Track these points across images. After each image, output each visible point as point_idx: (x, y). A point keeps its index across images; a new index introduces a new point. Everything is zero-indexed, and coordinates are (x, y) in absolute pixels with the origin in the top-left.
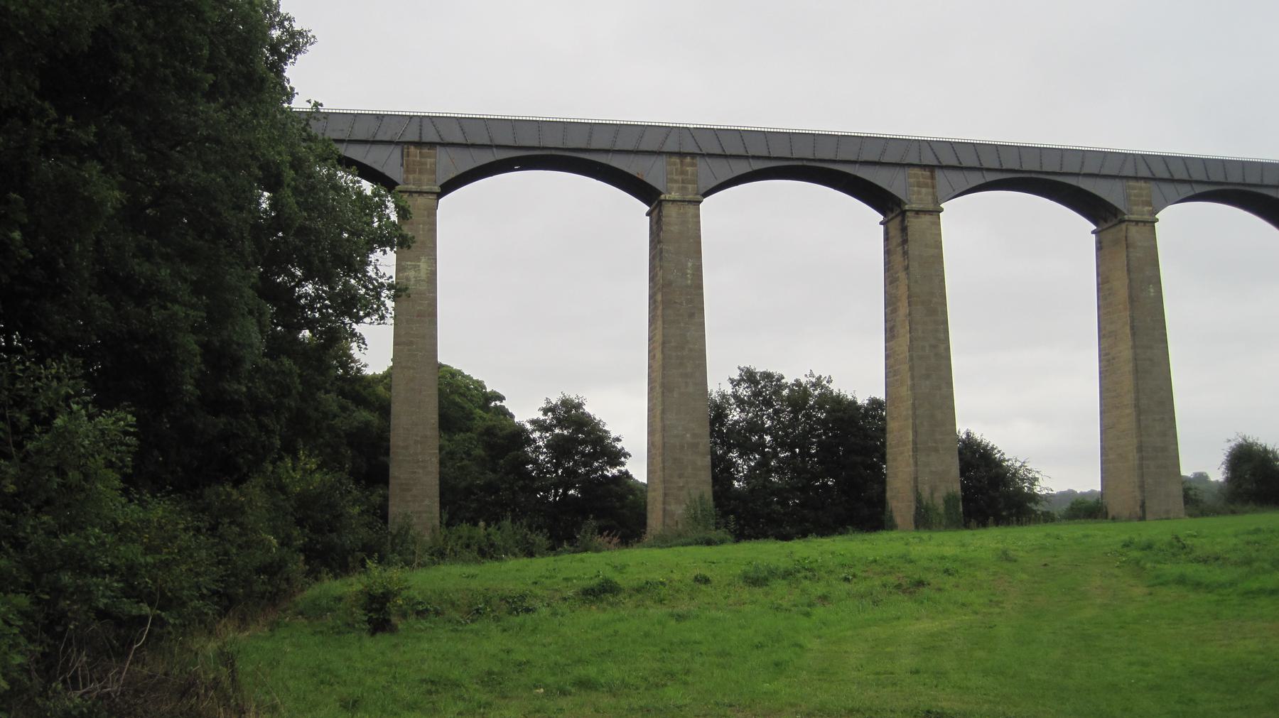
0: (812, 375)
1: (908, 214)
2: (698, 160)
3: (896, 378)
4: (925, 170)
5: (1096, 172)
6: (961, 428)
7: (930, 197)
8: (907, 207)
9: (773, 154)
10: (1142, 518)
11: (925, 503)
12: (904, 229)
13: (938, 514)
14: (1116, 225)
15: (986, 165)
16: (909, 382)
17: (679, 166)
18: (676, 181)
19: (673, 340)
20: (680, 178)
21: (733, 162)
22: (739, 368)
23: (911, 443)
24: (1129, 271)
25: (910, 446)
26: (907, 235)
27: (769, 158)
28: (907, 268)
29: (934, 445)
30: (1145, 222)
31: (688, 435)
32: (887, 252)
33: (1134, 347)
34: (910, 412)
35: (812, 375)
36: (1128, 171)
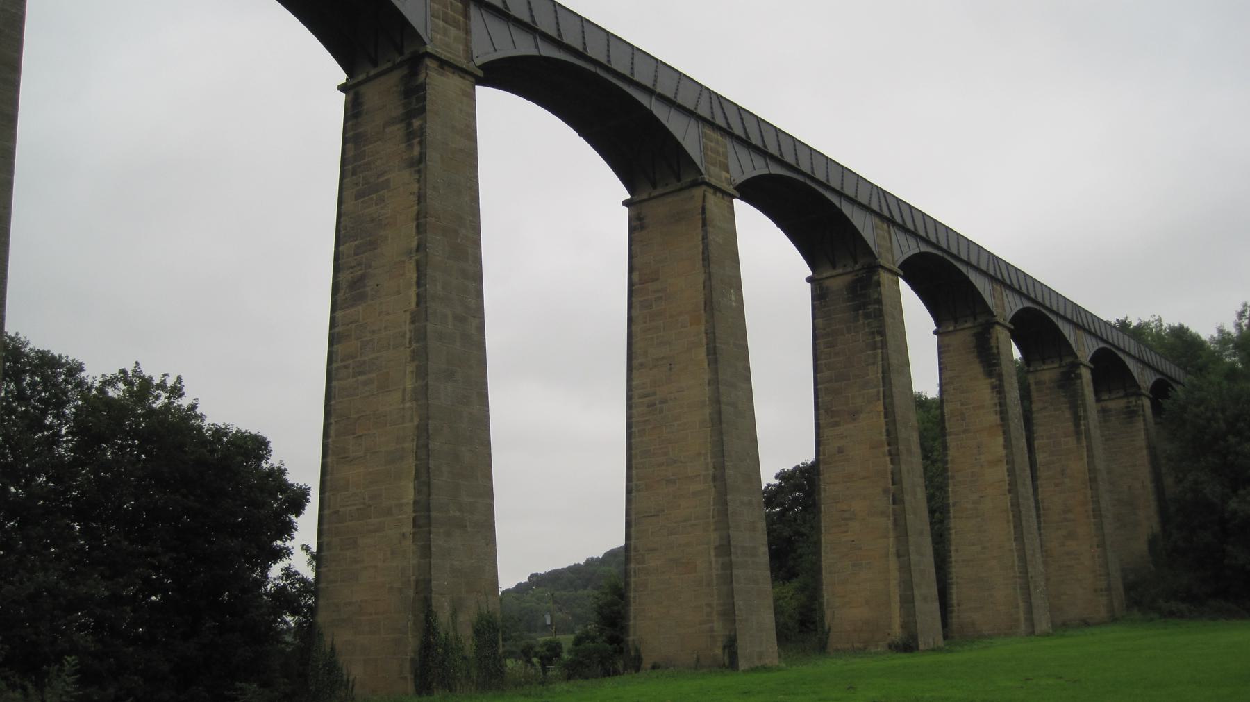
1: (428, 62)
3: (361, 378)
11: (443, 635)
13: (465, 658)
16: (409, 384)
24: (706, 259)
25: (409, 512)
28: (418, 164)
29: (458, 514)
30: (724, 193)
34: (410, 445)
36: (704, 111)
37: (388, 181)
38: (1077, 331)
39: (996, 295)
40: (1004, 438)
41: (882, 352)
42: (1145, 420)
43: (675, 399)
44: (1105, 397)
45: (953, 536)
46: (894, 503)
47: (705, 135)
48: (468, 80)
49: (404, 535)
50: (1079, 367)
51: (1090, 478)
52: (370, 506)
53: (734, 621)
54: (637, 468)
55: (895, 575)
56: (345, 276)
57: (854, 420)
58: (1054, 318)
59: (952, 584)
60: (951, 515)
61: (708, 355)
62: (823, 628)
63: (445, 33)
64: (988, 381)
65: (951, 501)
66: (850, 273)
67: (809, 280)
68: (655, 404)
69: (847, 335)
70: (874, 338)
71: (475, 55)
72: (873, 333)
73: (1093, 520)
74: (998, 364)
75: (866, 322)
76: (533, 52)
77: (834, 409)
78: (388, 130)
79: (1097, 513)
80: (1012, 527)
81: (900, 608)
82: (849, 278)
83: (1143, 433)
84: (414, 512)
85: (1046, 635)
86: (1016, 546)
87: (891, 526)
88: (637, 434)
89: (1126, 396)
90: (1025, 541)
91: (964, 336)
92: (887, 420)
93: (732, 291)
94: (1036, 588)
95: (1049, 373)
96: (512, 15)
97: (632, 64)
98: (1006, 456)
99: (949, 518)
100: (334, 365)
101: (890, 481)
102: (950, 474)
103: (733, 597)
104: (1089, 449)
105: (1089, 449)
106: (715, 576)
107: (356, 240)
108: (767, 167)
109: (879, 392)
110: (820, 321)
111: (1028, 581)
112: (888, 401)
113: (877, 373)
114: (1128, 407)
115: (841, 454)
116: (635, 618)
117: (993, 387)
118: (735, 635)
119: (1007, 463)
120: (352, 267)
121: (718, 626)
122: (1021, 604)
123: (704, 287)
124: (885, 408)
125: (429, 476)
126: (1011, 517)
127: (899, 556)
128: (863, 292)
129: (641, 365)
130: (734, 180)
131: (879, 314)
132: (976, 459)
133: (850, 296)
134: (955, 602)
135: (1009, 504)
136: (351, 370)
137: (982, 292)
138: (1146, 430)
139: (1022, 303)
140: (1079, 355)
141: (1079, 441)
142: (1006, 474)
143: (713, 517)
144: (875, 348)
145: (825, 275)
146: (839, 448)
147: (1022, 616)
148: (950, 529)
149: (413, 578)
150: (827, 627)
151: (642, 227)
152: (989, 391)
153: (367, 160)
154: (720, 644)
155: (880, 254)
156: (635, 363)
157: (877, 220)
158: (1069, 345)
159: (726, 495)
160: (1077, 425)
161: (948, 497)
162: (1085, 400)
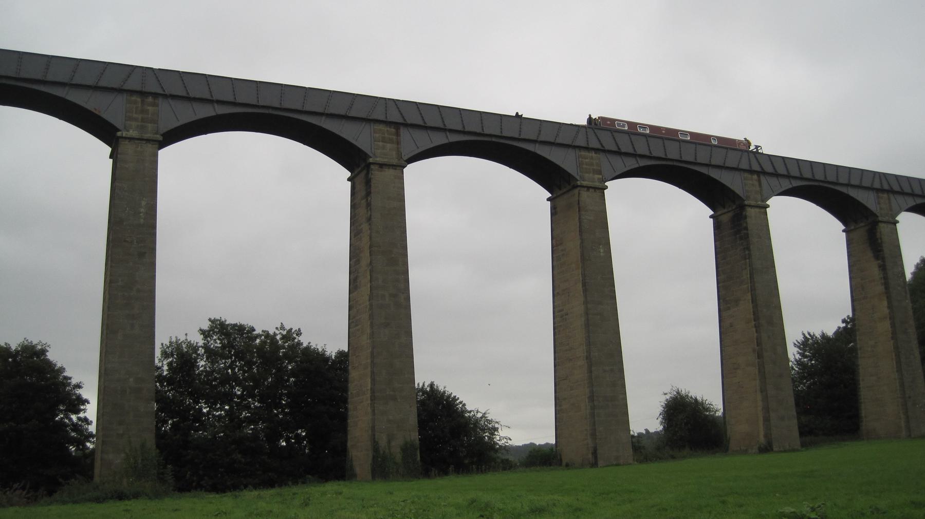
0: (282, 328)
1: (372, 167)
2: (160, 100)
3: (357, 328)
4: (390, 127)
5: (552, 140)
6: (422, 378)
7: (394, 153)
8: (371, 160)
9: (239, 100)
10: (594, 464)
11: (382, 452)
12: (368, 182)
15: (449, 127)
16: (369, 331)
17: (140, 105)
18: (136, 120)
19: (120, 279)
20: (140, 116)
21: (196, 105)
22: (210, 320)
23: (369, 392)
25: (369, 395)
26: (370, 186)
27: (234, 104)
28: (369, 219)
30: (595, 188)
31: (131, 380)
32: (353, 207)
33: (586, 302)
34: (369, 361)
35: (282, 328)
41: (749, 261)
60: (859, 356)
61: (582, 287)
71: (403, 155)
72: (744, 248)
77: (728, 299)
78: (362, 202)
82: (730, 214)
87: (757, 372)
93: (601, 246)
97: (520, 128)
101: (756, 343)
102: (857, 328)
110: (718, 243)
117: (880, 267)
119: (890, 318)
126: (894, 357)
127: (761, 392)
130: (605, 178)
131: (746, 237)
139: (915, 201)
144: (745, 259)
147: (903, 424)
150: (728, 436)
154: (591, 452)
157: (747, 175)
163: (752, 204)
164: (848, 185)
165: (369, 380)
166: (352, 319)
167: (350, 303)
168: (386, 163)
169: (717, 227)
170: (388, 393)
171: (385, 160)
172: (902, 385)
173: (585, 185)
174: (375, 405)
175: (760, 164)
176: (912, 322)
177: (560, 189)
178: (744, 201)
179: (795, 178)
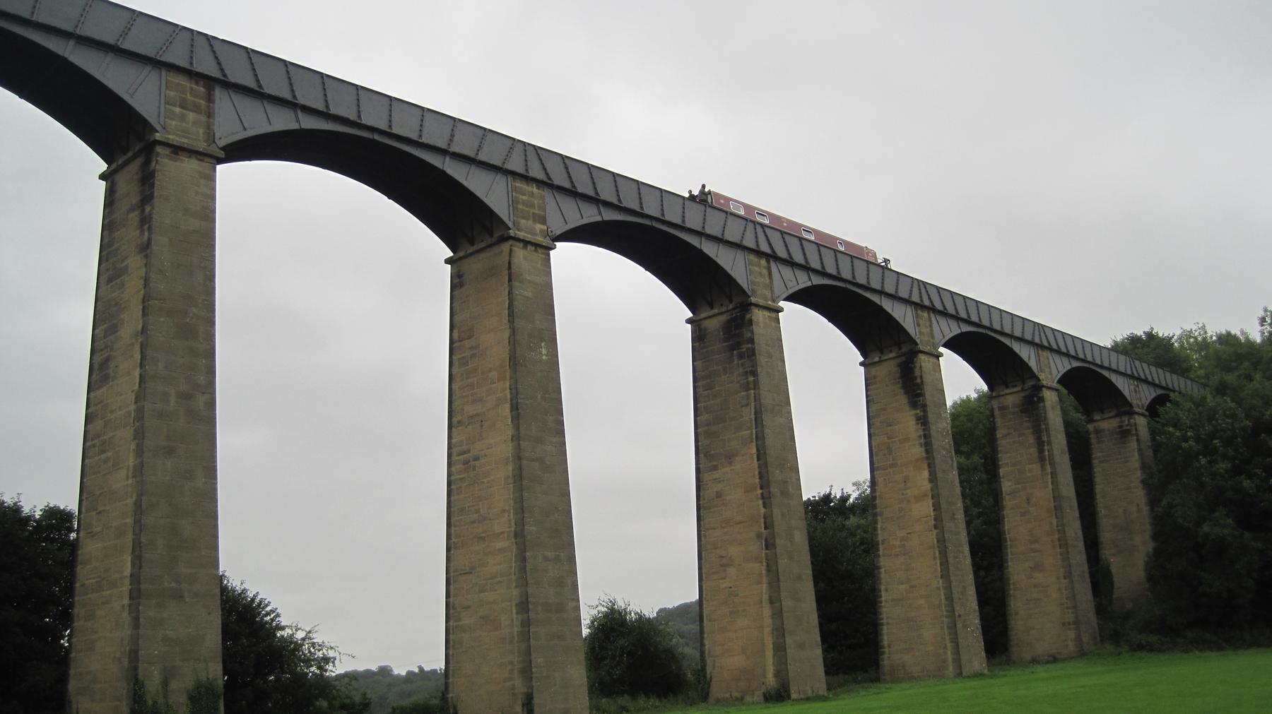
1: (159, 149)
3: (103, 456)
4: (197, 83)
7: (201, 131)
8: (158, 136)
11: (150, 703)
12: (147, 179)
14: (491, 245)
16: (131, 461)
23: (127, 581)
24: (511, 314)
25: (126, 588)
26: (152, 185)
28: (145, 248)
29: (173, 585)
30: (537, 246)
32: (109, 226)
33: (516, 438)
34: (130, 520)
36: (515, 164)
37: (127, 266)
38: (1040, 352)
39: (921, 322)
40: (929, 471)
41: (754, 393)
42: (1138, 440)
43: (486, 456)
44: (1097, 417)
45: (883, 576)
46: (767, 547)
47: (515, 189)
48: (207, 162)
49: (123, 606)
50: (1041, 390)
51: (1055, 507)
52: (103, 579)
53: (531, 678)
54: (455, 526)
55: (768, 621)
56: (98, 358)
57: (731, 463)
58: (1007, 341)
59: (882, 624)
60: (881, 553)
61: (511, 411)
62: (705, 676)
63: (182, 118)
64: (913, 412)
65: (880, 538)
66: (725, 312)
67: (689, 321)
68: (469, 462)
69: (723, 377)
70: (747, 379)
71: (217, 136)
73: (1059, 550)
74: (922, 395)
75: (740, 362)
76: (293, 126)
77: (712, 452)
79: (1063, 543)
80: (938, 564)
81: (774, 655)
82: (723, 318)
83: (1136, 454)
84: (131, 584)
85: (977, 675)
86: (943, 583)
87: (764, 572)
88: (455, 492)
89: (1119, 415)
90: (952, 578)
91: (889, 367)
92: (759, 462)
93: (543, 344)
94: (965, 627)
95: (1012, 398)
96: (266, 93)
98: (932, 490)
99: (879, 556)
100: (88, 444)
101: (763, 525)
102: (878, 510)
103: (530, 655)
104: (1054, 475)
105: (1054, 475)
106: (516, 633)
107: (105, 323)
108: (600, 214)
109: (752, 434)
110: (698, 363)
111: (955, 621)
112: (760, 442)
113: (750, 415)
114: (1121, 427)
115: (719, 499)
116: (453, 675)
117: (918, 419)
118: (532, 693)
120: (102, 350)
121: (518, 682)
122: (949, 645)
123: (509, 342)
124: (758, 450)
125: (141, 551)
126: (937, 555)
127: (771, 602)
128: (737, 331)
129: (459, 422)
131: (752, 353)
132: (903, 494)
133: (726, 336)
134: (885, 643)
135: (935, 540)
136: (97, 449)
137: (900, 321)
138: (1140, 450)
140: (1041, 378)
141: (1043, 467)
142: (932, 508)
143: (515, 574)
144: (748, 389)
145: (703, 315)
146: (717, 492)
147: (949, 656)
148: (879, 568)
149: (127, 648)
150: (708, 677)
151: (461, 285)
152: (914, 422)
153: (116, 246)
154: (520, 702)
155: (754, 291)
156: (455, 420)
157: (752, 257)
158: (1029, 368)
159: (525, 552)
160: (1041, 451)
161: (877, 534)
162: (1048, 423)
163: (761, 304)
164: (881, 293)
165: (128, 559)
166: (92, 440)
167: (90, 410)
168: (186, 146)
169: (699, 338)
170: (166, 584)
171: (184, 141)
172: (950, 598)
173: (521, 238)
174: (140, 608)
175: (770, 244)
176: (960, 504)
177: (472, 244)
178: (749, 297)
179: (815, 271)
